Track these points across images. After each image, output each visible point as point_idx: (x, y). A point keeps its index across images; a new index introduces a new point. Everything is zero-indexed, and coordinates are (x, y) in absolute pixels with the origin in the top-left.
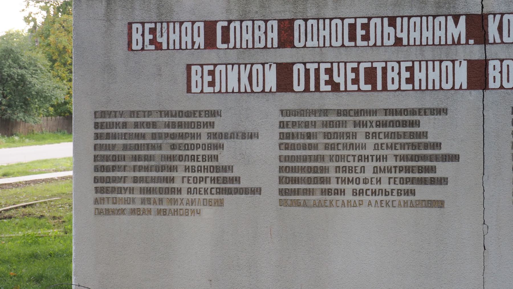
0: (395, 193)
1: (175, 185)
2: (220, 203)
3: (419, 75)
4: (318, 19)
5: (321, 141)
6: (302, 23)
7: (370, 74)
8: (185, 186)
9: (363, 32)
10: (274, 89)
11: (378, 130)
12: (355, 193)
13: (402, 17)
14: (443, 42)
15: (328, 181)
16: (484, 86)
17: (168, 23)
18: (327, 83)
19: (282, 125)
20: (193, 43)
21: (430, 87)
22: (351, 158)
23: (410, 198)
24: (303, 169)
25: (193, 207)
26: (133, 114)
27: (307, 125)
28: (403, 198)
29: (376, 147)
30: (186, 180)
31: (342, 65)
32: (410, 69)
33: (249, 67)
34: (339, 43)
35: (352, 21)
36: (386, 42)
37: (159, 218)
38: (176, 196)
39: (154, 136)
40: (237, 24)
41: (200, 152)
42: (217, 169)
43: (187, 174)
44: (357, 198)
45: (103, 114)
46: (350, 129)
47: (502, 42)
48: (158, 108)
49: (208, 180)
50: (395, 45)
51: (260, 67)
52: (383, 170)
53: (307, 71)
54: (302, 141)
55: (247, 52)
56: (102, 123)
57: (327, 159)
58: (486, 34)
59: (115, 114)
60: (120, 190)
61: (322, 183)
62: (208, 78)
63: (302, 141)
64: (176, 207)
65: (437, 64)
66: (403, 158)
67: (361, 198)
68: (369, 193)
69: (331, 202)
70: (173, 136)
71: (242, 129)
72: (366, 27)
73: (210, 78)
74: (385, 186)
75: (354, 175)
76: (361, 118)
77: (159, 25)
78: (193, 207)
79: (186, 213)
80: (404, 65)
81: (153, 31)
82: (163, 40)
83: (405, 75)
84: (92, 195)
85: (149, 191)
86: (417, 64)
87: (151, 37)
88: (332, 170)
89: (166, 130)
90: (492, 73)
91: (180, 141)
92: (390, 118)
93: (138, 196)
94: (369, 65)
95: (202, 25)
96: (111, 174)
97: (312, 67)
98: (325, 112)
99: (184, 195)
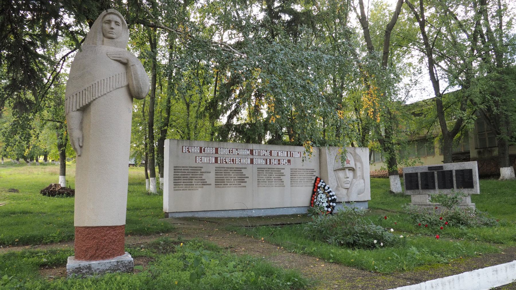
2: (202, 187)
3: (242, 161)
5: (223, 174)
7: (233, 160)
8: (195, 183)
12: (230, 184)
15: (225, 182)
16: (253, 164)
24: (220, 180)
26: (183, 167)
27: (221, 170)
29: (234, 175)
32: (240, 160)
37: (189, 191)
39: (188, 172)
41: (198, 176)
42: (202, 180)
45: (176, 167)
46: (229, 171)
52: (235, 180)
66: (239, 177)
70: (192, 172)
72: (232, 150)
74: (235, 183)
79: (195, 190)
81: (188, 148)
82: (190, 150)
83: (239, 161)
84: (173, 186)
85: (187, 185)
90: (254, 161)
93: (184, 186)
97: (222, 158)
98: (224, 168)
99: (195, 186)
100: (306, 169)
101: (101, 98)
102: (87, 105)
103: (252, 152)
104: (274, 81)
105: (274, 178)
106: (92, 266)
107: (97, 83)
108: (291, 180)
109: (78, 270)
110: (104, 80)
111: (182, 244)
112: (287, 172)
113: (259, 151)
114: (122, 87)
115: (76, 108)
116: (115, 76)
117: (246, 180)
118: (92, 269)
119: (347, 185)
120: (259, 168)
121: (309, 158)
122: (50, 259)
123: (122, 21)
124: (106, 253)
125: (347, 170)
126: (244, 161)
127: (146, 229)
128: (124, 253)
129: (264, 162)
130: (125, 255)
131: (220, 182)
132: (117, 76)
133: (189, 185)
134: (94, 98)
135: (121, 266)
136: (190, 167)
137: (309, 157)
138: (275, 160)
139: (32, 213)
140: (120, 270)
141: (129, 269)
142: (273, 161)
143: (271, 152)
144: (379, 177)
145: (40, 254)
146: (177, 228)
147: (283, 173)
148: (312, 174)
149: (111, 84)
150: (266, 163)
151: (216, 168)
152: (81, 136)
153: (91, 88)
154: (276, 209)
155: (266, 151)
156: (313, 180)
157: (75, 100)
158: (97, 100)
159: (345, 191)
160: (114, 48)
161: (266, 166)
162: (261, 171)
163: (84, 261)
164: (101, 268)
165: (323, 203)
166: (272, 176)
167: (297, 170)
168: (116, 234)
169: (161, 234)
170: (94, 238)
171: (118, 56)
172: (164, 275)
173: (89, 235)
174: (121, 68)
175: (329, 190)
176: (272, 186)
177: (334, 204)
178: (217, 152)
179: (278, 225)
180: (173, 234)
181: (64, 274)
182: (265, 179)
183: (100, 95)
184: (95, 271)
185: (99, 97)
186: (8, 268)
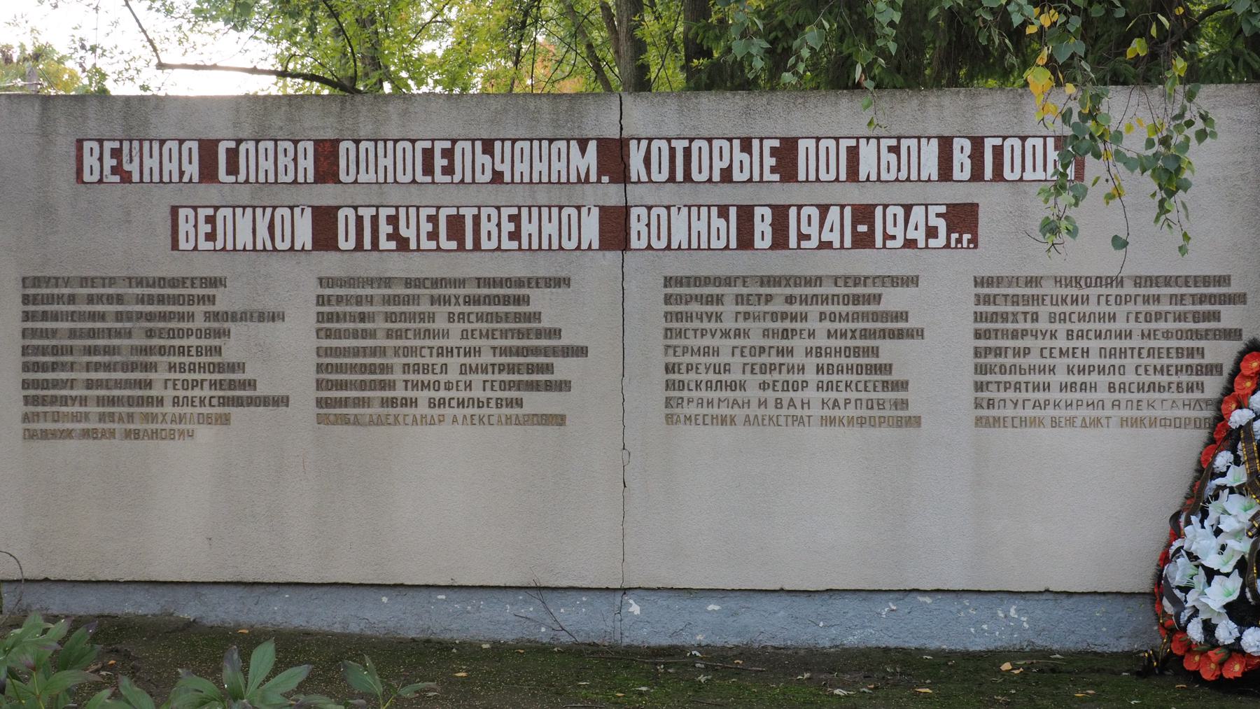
0: (493, 403)
1: (153, 393)
2: (225, 420)
3: (527, 228)
4: (376, 141)
5: (381, 325)
6: (351, 146)
7: (455, 226)
8: (170, 393)
9: (445, 162)
10: (309, 246)
11: (467, 309)
12: (432, 403)
13: (503, 140)
14: (563, 179)
15: (391, 385)
16: (624, 245)
17: (141, 141)
18: (390, 237)
19: (321, 300)
20: (182, 173)
21: (545, 246)
22: (426, 352)
23: (516, 411)
24: (353, 368)
25: (182, 426)
26: (84, 281)
27: (359, 300)
28: (506, 411)
29: (464, 334)
30: (170, 384)
31: (412, 211)
32: (515, 219)
33: (269, 211)
34: (409, 178)
35: (428, 145)
36: (479, 178)
37: (129, 444)
38: (155, 410)
39: (119, 316)
40: (251, 145)
41: (193, 341)
42: (220, 368)
43: (173, 376)
44: (436, 411)
45: (37, 281)
46: (425, 307)
47: (650, 181)
48: (125, 274)
49: (206, 385)
50: (492, 182)
51: (287, 212)
52: (474, 370)
53: (359, 220)
54: (351, 326)
55: (266, 188)
56: (35, 296)
57: (390, 352)
58: (626, 167)
59: (56, 281)
60: (64, 401)
61: (383, 388)
62: (205, 228)
63: (351, 326)
64: (154, 426)
65: (555, 211)
66: (505, 351)
67: (442, 411)
68: (454, 403)
69: (396, 417)
70: (150, 317)
71: (259, 307)
72: (448, 154)
73: (208, 228)
74: (477, 393)
75: (430, 377)
76: (443, 291)
77: (126, 145)
78: (182, 426)
79: (171, 435)
80: (506, 212)
81: (116, 153)
82: (133, 168)
83: (508, 227)
84: (20, 408)
85: (112, 401)
86: (525, 211)
87: (114, 162)
88: (398, 369)
89: (139, 308)
90: (635, 226)
91: (161, 325)
92: (485, 291)
93: (93, 409)
94: (453, 211)
95: (195, 146)
96: (50, 376)
97: (367, 213)
98: (387, 282)
99: (168, 409)
100: (1138, 281)
105: (819, 352)
108: (980, 370)
113: (680, 145)
117: (564, 368)
120: (679, 281)
126: (550, 228)
129: (725, 231)
136: (130, 281)
138: (824, 209)
142: (804, 221)
143: (786, 156)
147: (902, 316)
148: (1197, 317)
150: (746, 240)
154: (838, 603)
161: (742, 263)
162: (699, 299)
165: (1211, 574)
166: (798, 344)
167: (1048, 289)
176: (799, 421)
178: (327, 170)
182: (737, 360)
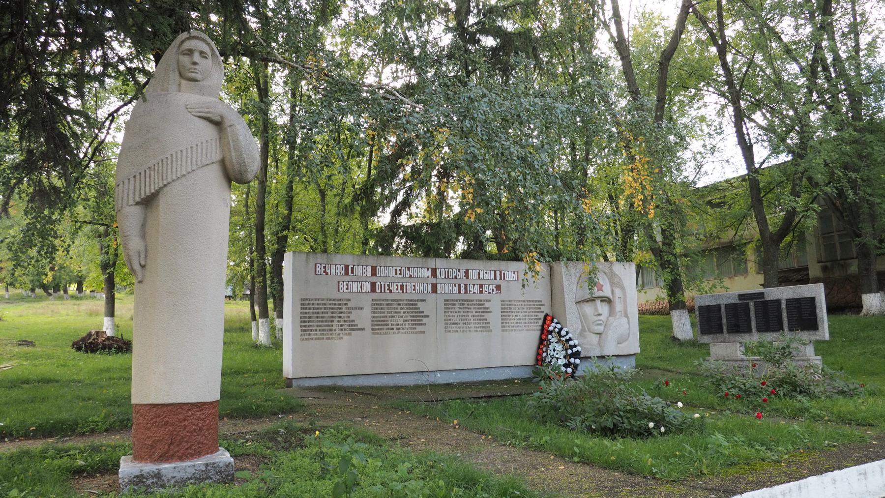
1: (334, 328)
2: (350, 334)
3: (417, 288)
7: (402, 286)
12: (397, 329)
15: (388, 325)
16: (436, 293)
24: (380, 321)
26: (316, 300)
27: (381, 304)
29: (404, 312)
32: (414, 286)
39: (325, 309)
41: (343, 315)
42: (349, 321)
45: (305, 300)
46: (395, 306)
52: (406, 321)
70: (332, 309)
72: (400, 270)
74: (407, 326)
79: (337, 338)
81: (325, 267)
82: (329, 271)
83: (413, 288)
85: (323, 330)
93: (318, 332)
96: (307, 324)
97: (383, 284)
98: (387, 300)
99: (337, 332)
100: (528, 301)
101: (177, 183)
102: (152, 194)
103: (434, 272)
104: (472, 149)
106: (164, 472)
107: (169, 157)
108: (502, 319)
109: (139, 479)
110: (181, 151)
111: (317, 432)
112: (495, 306)
113: (447, 270)
114: (213, 163)
115: (134, 201)
116: (200, 145)
117: (425, 320)
118: (163, 478)
119: (599, 327)
120: (447, 300)
121: (534, 282)
122: (90, 460)
123: (212, 50)
124: (187, 449)
125: (598, 302)
127: (254, 408)
128: (218, 450)
129: (456, 289)
130: (219, 453)
131: (379, 325)
132: (204, 145)
133: (327, 331)
134: (165, 182)
135: (213, 472)
136: (328, 300)
137: (534, 279)
138: (474, 285)
139: (57, 381)
140: (211, 478)
141: (227, 477)
143: (467, 272)
144: (653, 313)
145: (72, 452)
146: (308, 406)
147: (488, 308)
148: (537, 308)
149: (194, 160)
150: (460, 292)
151: (373, 300)
152: (142, 248)
153: (160, 165)
155: (459, 271)
156: (540, 319)
157: (132, 187)
158: (169, 187)
159: (594, 339)
160: (198, 97)
161: (458, 297)
163: (149, 464)
164: (179, 476)
165: (557, 359)
166: (470, 314)
167: (513, 303)
168: (203, 417)
169: (280, 416)
170: (167, 423)
171: (206, 110)
172: (287, 487)
173: (158, 419)
174: (210, 131)
175: (567, 337)
177: (578, 361)
178: (374, 273)
179: (482, 397)
180: (301, 415)
181: (114, 487)
183: (174, 178)
184: (168, 481)
185: (173, 181)
186: (18, 476)
